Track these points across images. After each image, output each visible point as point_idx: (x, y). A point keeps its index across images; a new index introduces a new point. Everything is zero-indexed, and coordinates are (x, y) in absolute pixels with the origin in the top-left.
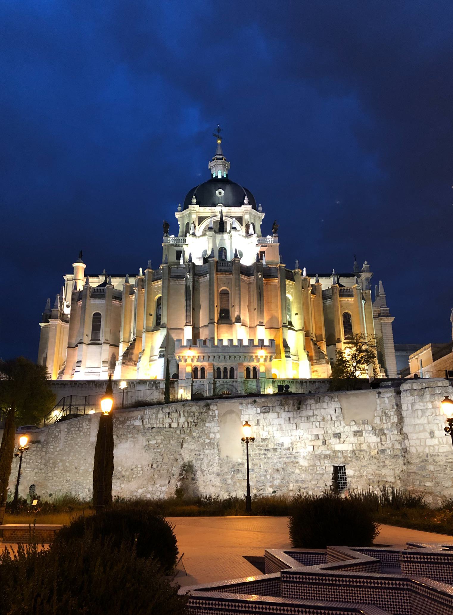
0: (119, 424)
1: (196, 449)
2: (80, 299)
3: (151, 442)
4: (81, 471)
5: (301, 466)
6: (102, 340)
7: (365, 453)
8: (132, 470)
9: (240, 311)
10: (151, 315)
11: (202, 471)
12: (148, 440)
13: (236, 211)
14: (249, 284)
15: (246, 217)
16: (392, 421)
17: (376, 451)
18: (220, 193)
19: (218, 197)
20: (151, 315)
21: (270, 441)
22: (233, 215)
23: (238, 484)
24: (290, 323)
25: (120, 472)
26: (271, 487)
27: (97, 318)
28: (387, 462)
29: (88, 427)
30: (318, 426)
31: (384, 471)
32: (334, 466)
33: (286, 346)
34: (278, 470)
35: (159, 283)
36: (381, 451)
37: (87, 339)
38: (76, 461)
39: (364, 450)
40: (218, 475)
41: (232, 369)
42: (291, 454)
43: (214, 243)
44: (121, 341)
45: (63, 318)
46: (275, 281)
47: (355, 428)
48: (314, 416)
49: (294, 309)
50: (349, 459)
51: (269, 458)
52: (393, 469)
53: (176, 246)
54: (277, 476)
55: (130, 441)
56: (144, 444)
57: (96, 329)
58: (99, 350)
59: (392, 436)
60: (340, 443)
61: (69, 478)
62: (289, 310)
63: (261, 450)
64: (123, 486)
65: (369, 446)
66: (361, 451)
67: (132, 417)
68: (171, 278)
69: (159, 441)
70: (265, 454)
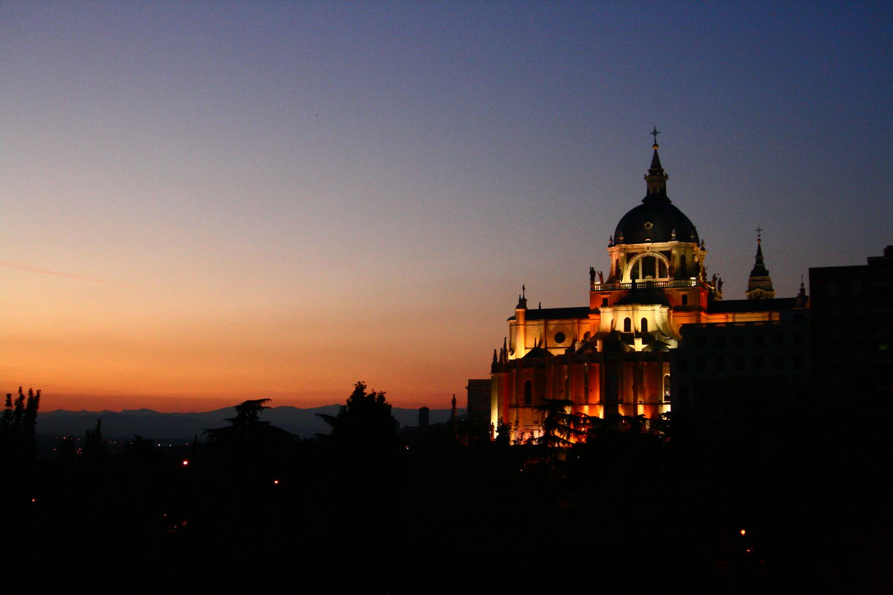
9: (623, 395)
15: (674, 252)
27: (528, 384)
53: (602, 294)
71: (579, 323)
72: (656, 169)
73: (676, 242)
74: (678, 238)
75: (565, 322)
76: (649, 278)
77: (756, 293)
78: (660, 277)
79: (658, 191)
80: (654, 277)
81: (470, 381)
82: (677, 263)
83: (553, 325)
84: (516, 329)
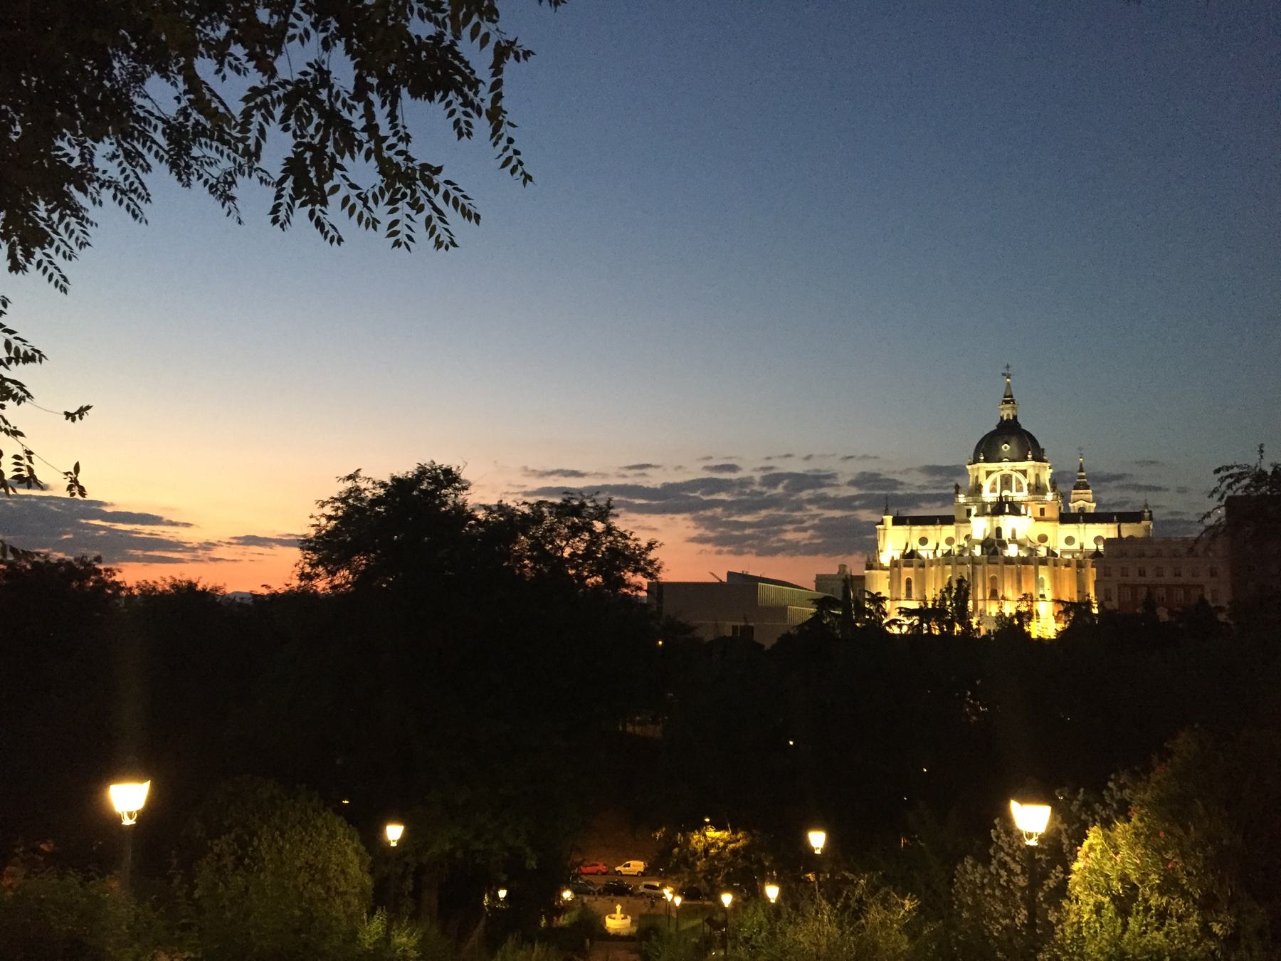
2: (896, 566)
6: (914, 596)
13: (1021, 465)
14: (1012, 570)
15: (1031, 472)
18: (1006, 448)
19: (1004, 452)
22: (1018, 468)
24: (1042, 596)
27: (909, 582)
33: (1038, 615)
35: (950, 567)
37: (903, 597)
43: (992, 525)
45: (883, 568)
46: (1033, 567)
49: (1047, 584)
53: (966, 505)
57: (909, 589)
62: (1043, 586)
68: (959, 564)
71: (941, 529)
72: (1009, 399)
73: (1033, 463)
74: (1034, 459)
75: (930, 527)
76: (1005, 493)
77: (1079, 505)
78: (1017, 491)
79: (1011, 418)
80: (1011, 492)
81: (817, 575)
82: (1033, 481)
83: (918, 531)
84: (884, 535)
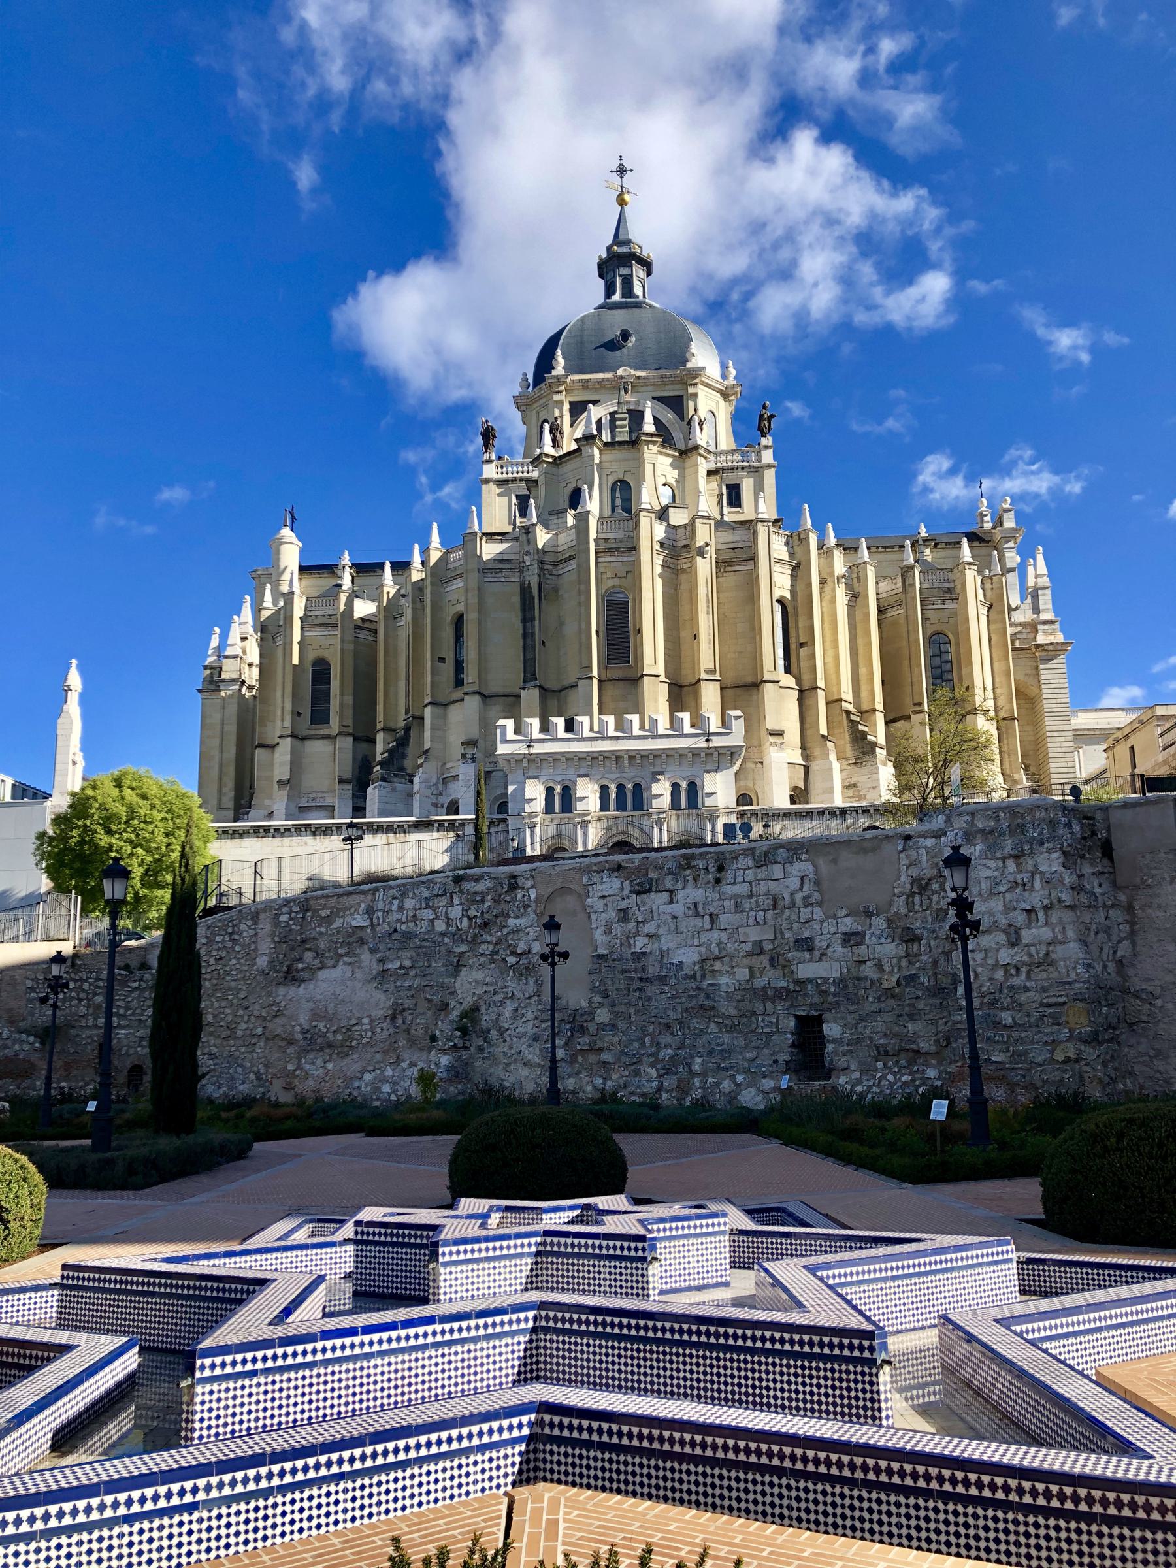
0: (320, 925)
1: (488, 980)
3: (389, 966)
4: (239, 1033)
5: (723, 1016)
7: (868, 984)
8: (349, 1030)
10: (442, 660)
11: (502, 1032)
12: (382, 961)
16: (935, 906)
17: (895, 979)
20: (442, 660)
21: (652, 959)
23: (580, 1059)
25: (324, 1036)
26: (652, 1065)
28: (921, 1005)
29: (252, 932)
30: (760, 920)
31: (911, 1027)
32: (797, 1016)
34: (668, 1026)
36: (905, 978)
38: (228, 1011)
39: (866, 978)
40: (535, 1040)
41: (637, 787)
42: (698, 989)
44: (379, 726)
47: (848, 924)
48: (751, 896)
50: (831, 999)
51: (649, 999)
52: (934, 1022)
54: (665, 1039)
55: (345, 963)
56: (376, 968)
58: (331, 748)
59: (933, 943)
60: (811, 960)
61: (214, 1050)
63: (632, 979)
64: (330, 1066)
65: (879, 966)
66: (859, 979)
67: (346, 909)
69: (407, 963)
70: (640, 990)
